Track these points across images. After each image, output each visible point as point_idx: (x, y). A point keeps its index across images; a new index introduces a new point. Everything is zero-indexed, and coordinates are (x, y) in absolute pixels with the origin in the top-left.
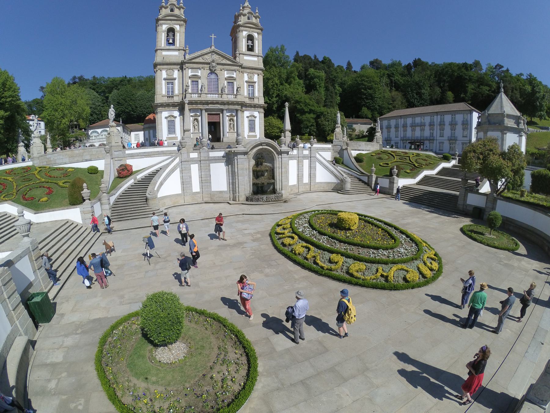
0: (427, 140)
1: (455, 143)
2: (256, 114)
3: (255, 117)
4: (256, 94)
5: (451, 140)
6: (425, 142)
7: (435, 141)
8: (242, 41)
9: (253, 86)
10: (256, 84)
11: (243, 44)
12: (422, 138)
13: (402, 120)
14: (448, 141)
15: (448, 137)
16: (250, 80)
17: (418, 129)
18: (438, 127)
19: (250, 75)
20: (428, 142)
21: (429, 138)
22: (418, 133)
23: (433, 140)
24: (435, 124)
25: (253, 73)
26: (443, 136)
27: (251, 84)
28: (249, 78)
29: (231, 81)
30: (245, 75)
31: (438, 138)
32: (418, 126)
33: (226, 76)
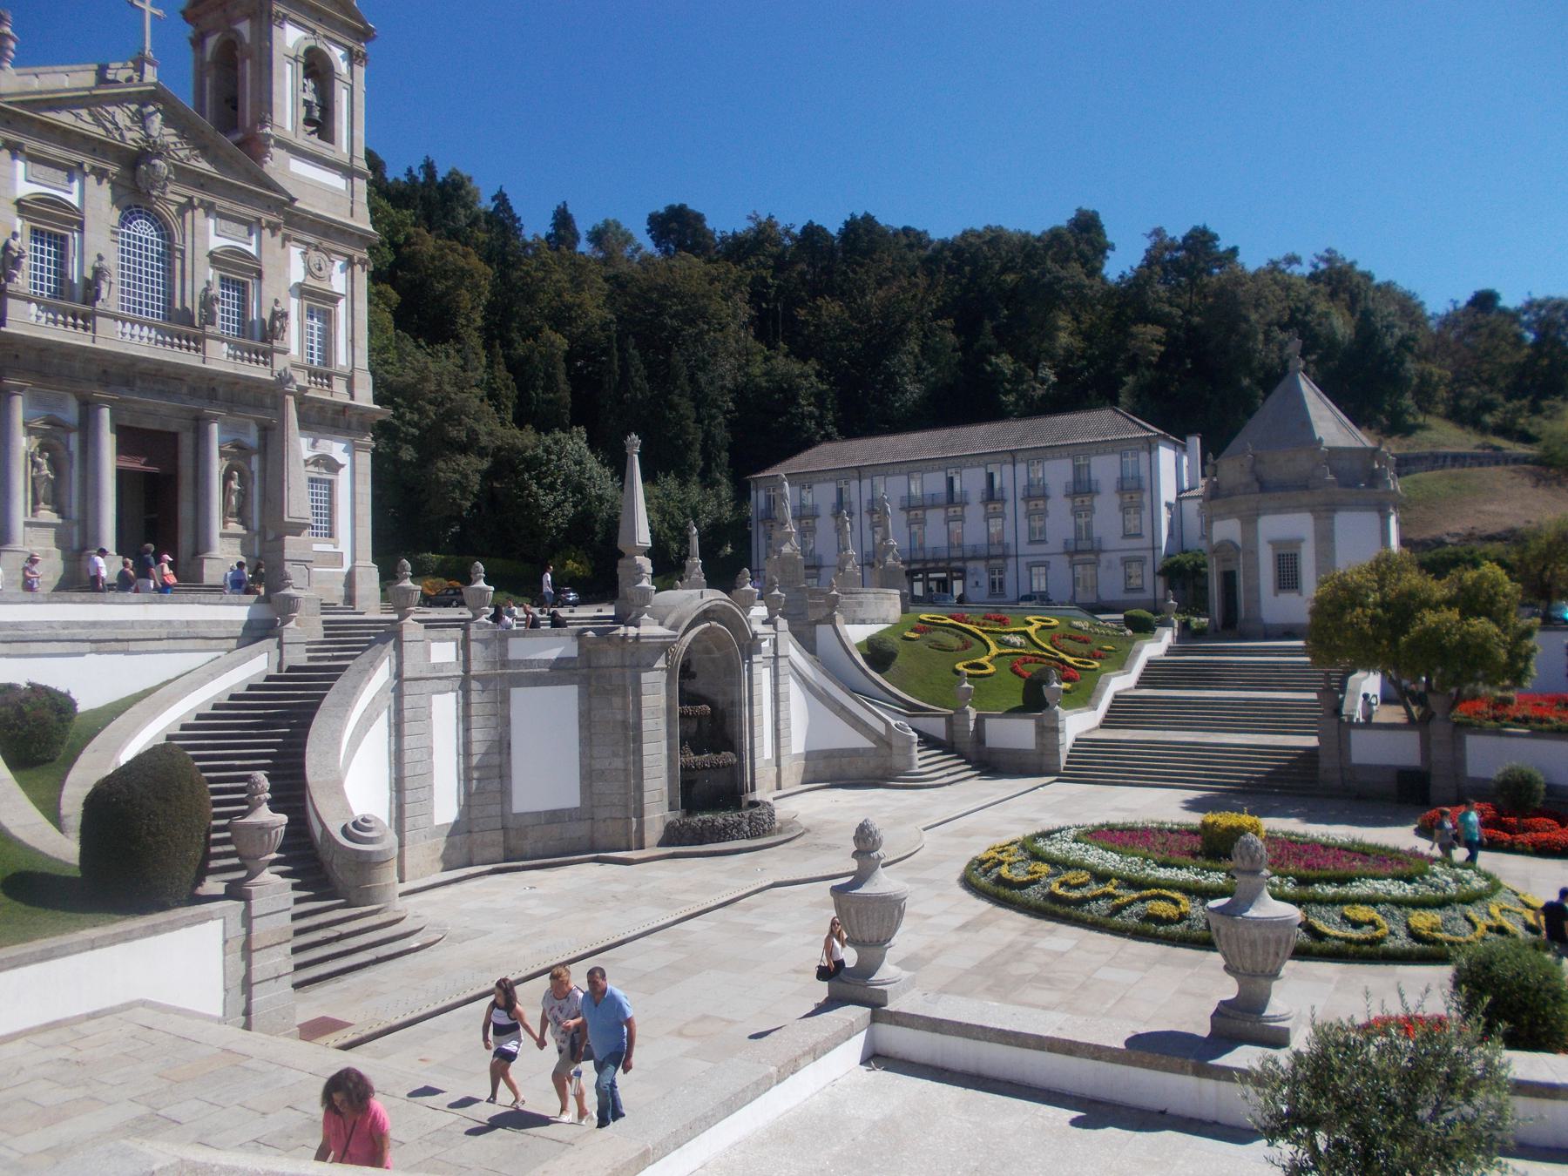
0: (974, 558)
1: (1096, 563)
2: (337, 449)
3: (334, 466)
4: (342, 359)
5: (1077, 552)
6: (970, 565)
7: (1011, 562)
8: (283, 75)
9: (327, 318)
10: (342, 307)
11: (288, 93)
12: (956, 553)
13: (866, 483)
14: (1066, 558)
15: (1066, 542)
16: (312, 282)
17: (935, 517)
18: (1022, 507)
19: (315, 256)
20: (981, 565)
21: (984, 552)
22: (935, 533)
23: (1005, 556)
24: (1009, 494)
25: (328, 252)
26: (1043, 541)
27: (319, 302)
28: (309, 272)
29: (240, 273)
30: (295, 252)
31: (1024, 548)
32: (933, 506)
33: (216, 243)
